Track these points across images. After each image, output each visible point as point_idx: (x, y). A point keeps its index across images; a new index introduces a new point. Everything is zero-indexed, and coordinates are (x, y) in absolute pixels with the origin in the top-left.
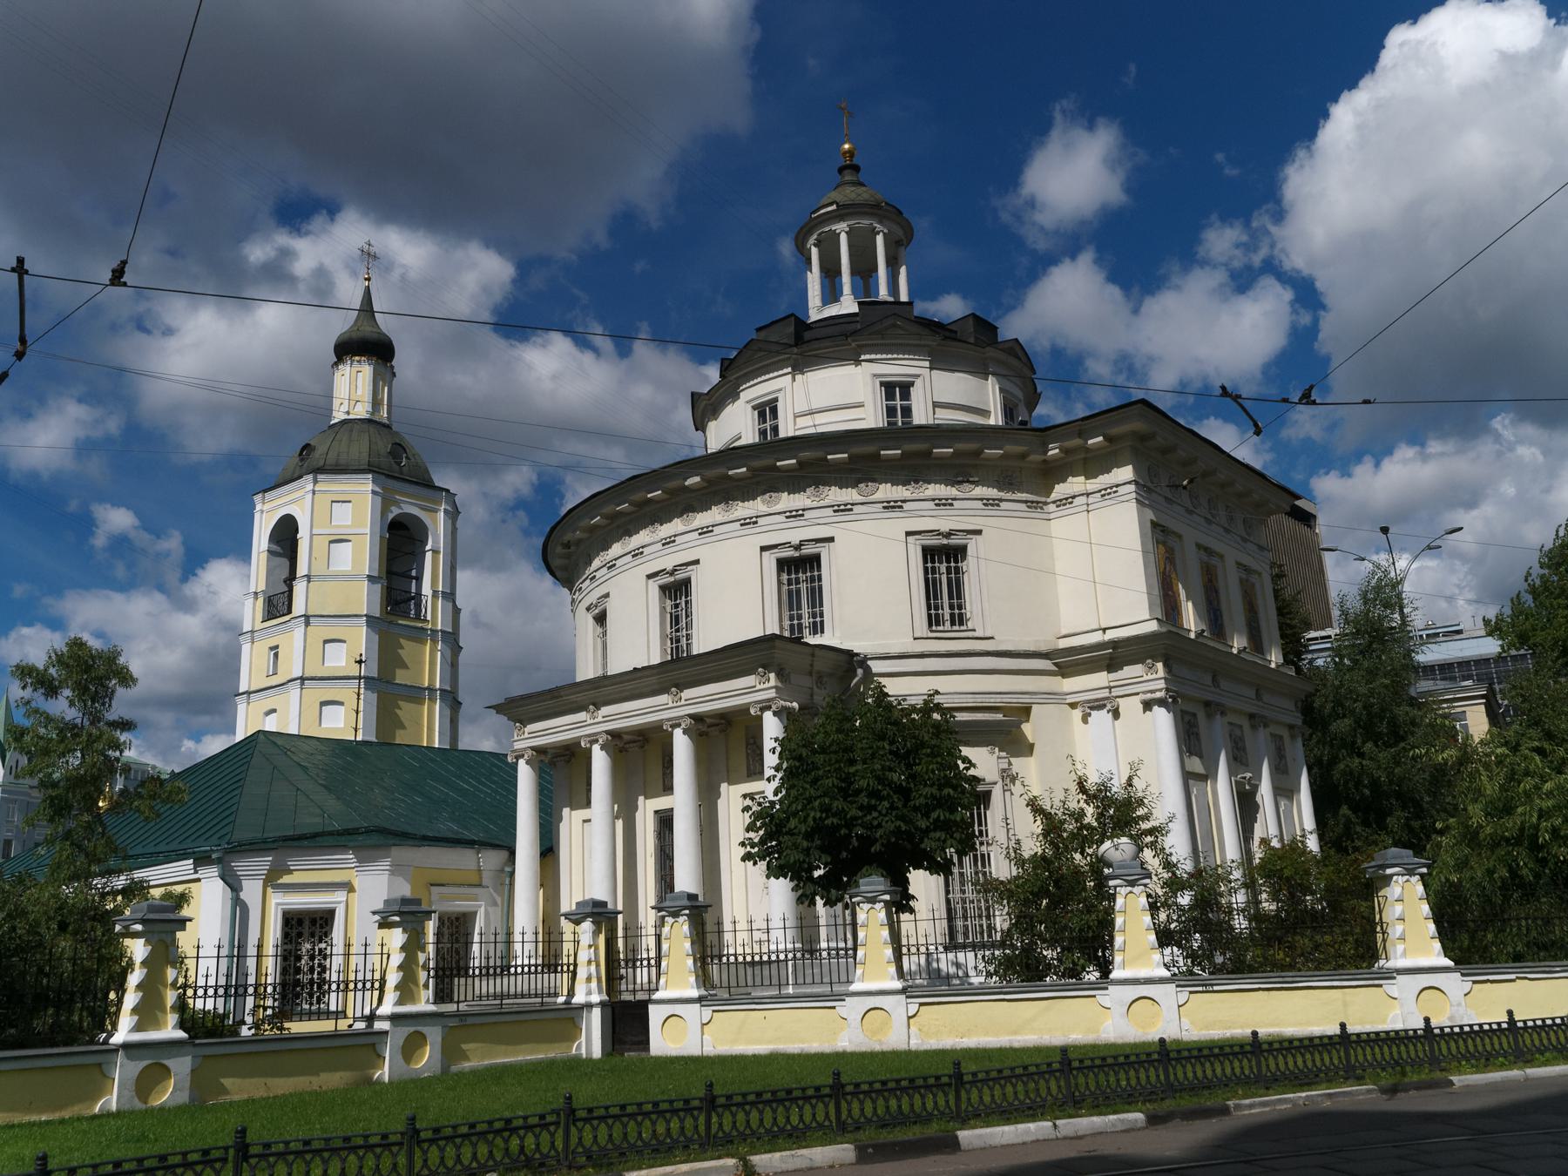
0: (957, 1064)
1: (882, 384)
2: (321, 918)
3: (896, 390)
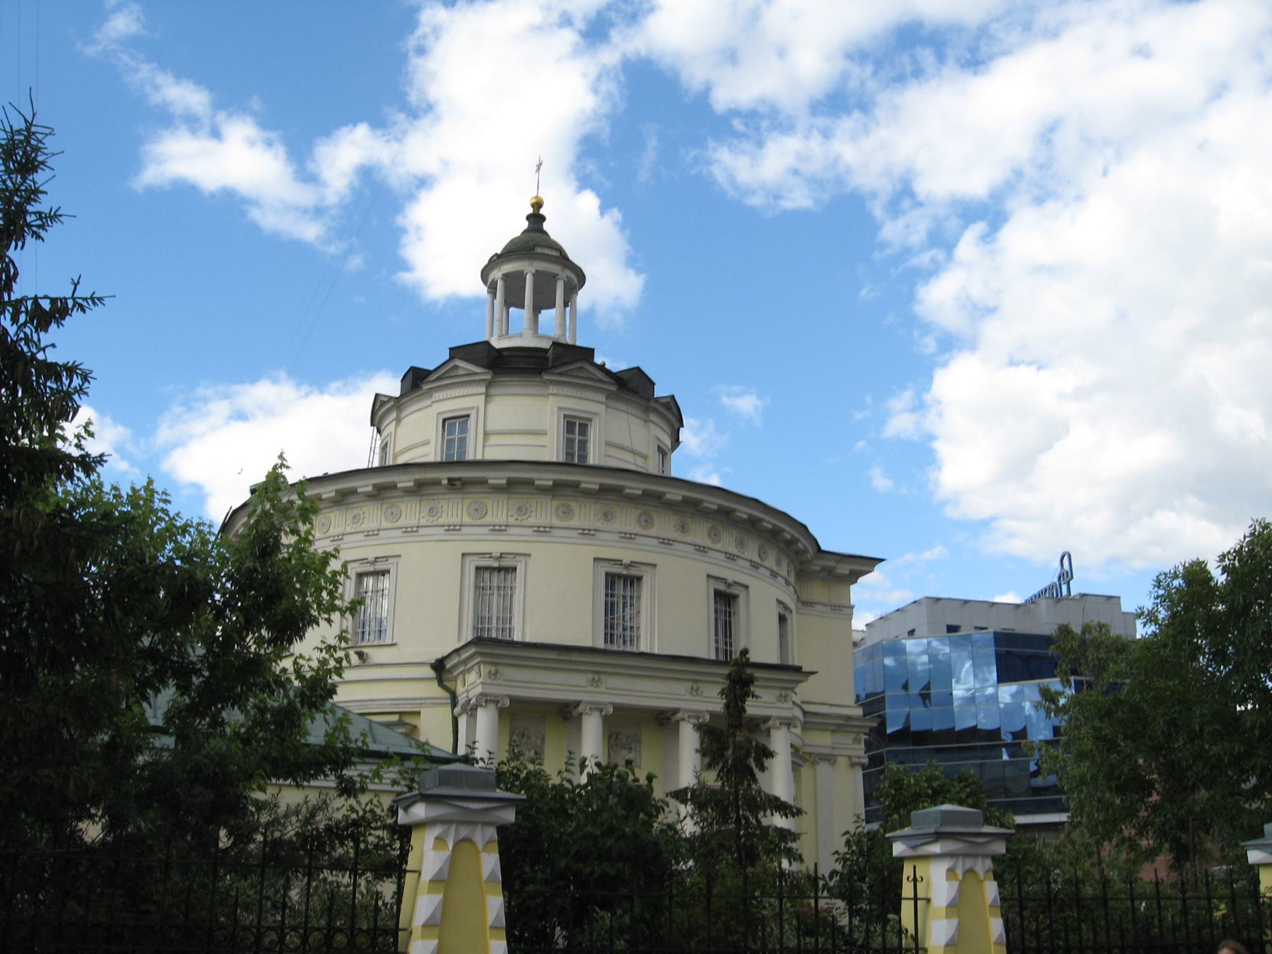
1: (565, 416)
3: (575, 427)
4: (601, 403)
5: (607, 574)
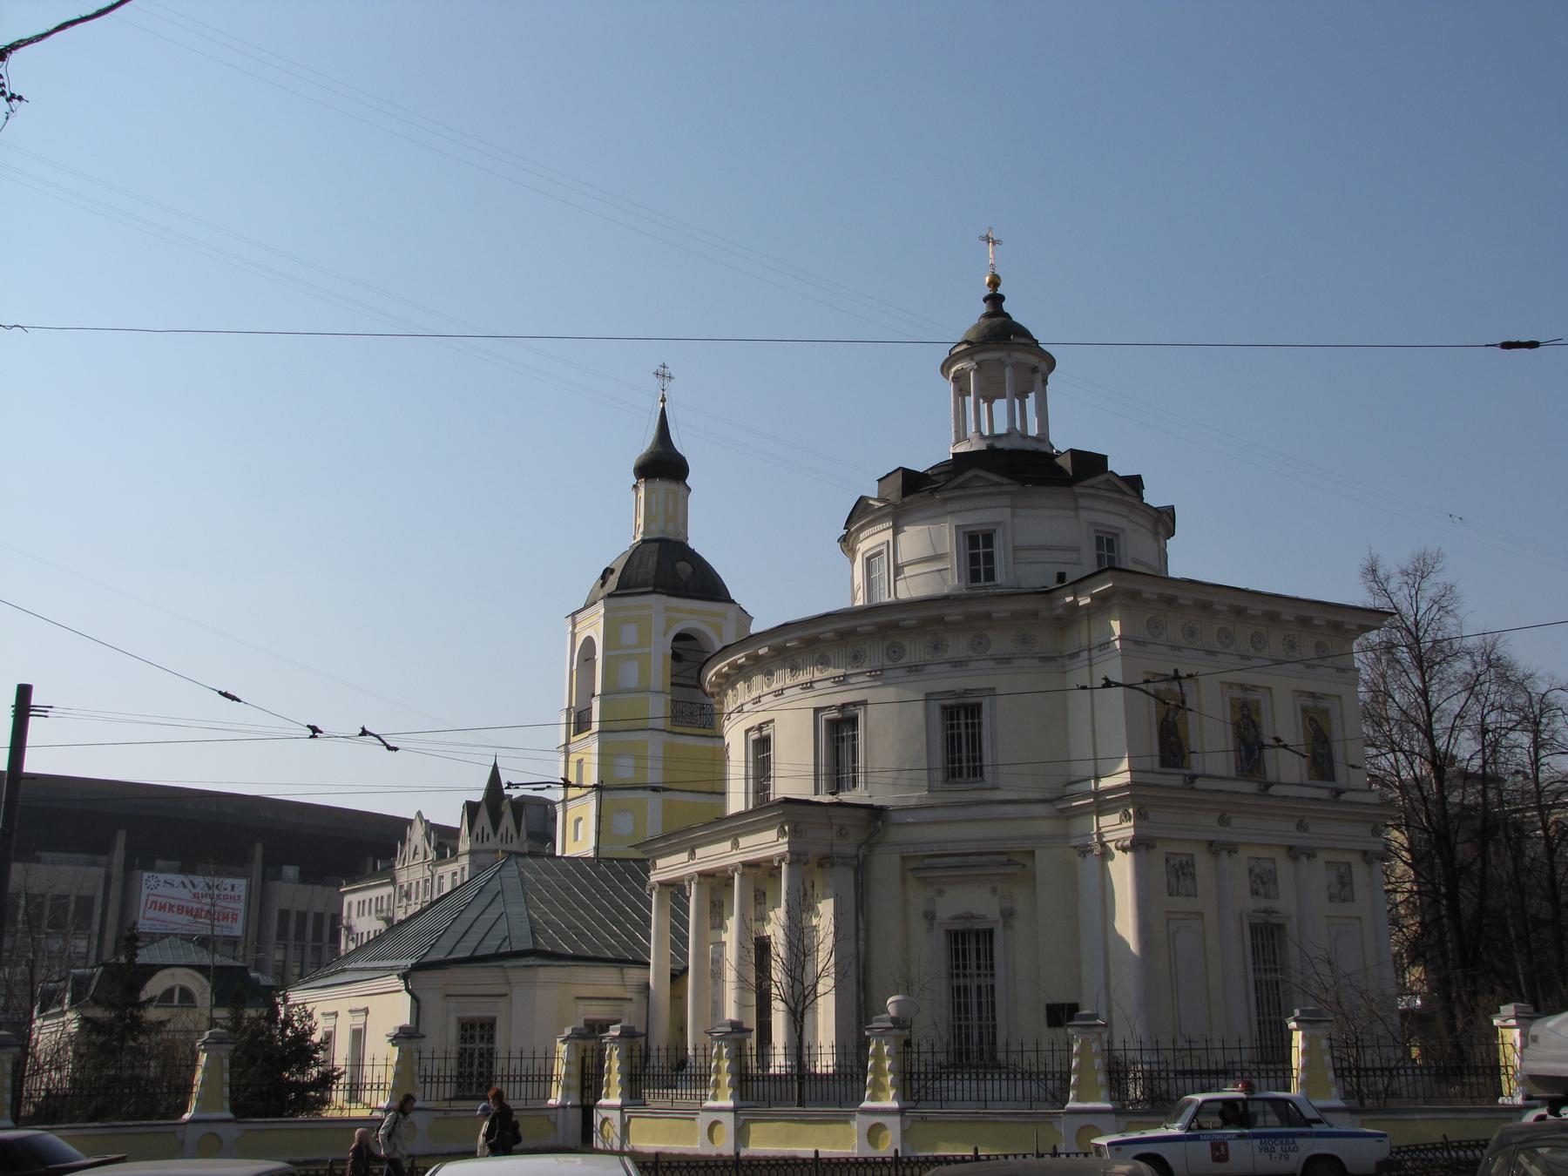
4: (1005, 507)
5: (944, 708)
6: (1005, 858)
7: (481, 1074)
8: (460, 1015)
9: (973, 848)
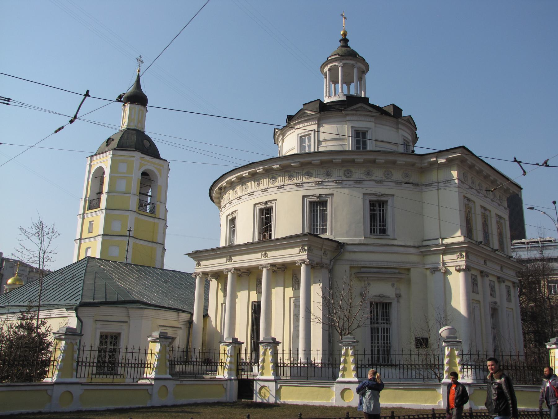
0: (393, 412)
1: (355, 130)
2: (115, 336)
4: (373, 122)
5: (370, 201)
6: (397, 271)
7: (109, 362)
8: (102, 331)
9: (385, 265)
